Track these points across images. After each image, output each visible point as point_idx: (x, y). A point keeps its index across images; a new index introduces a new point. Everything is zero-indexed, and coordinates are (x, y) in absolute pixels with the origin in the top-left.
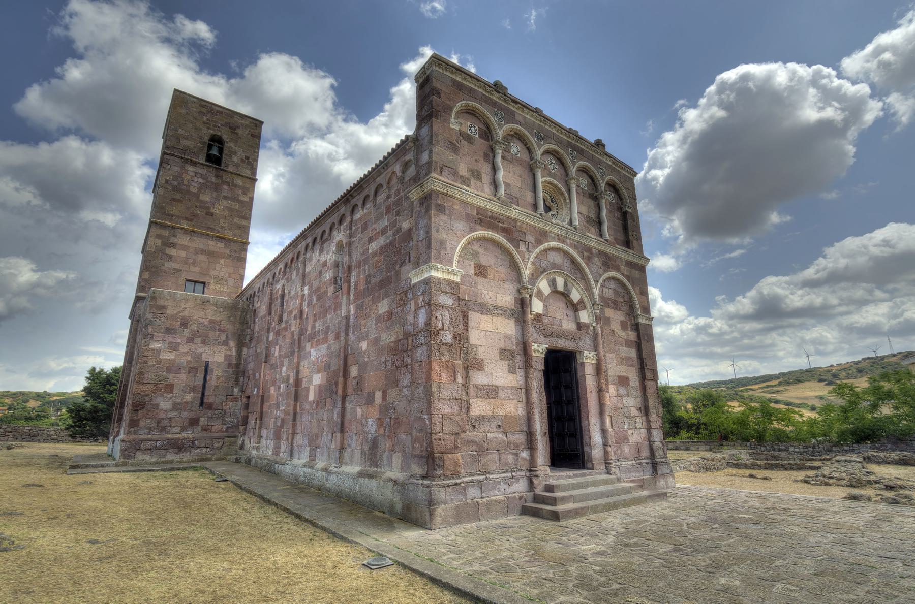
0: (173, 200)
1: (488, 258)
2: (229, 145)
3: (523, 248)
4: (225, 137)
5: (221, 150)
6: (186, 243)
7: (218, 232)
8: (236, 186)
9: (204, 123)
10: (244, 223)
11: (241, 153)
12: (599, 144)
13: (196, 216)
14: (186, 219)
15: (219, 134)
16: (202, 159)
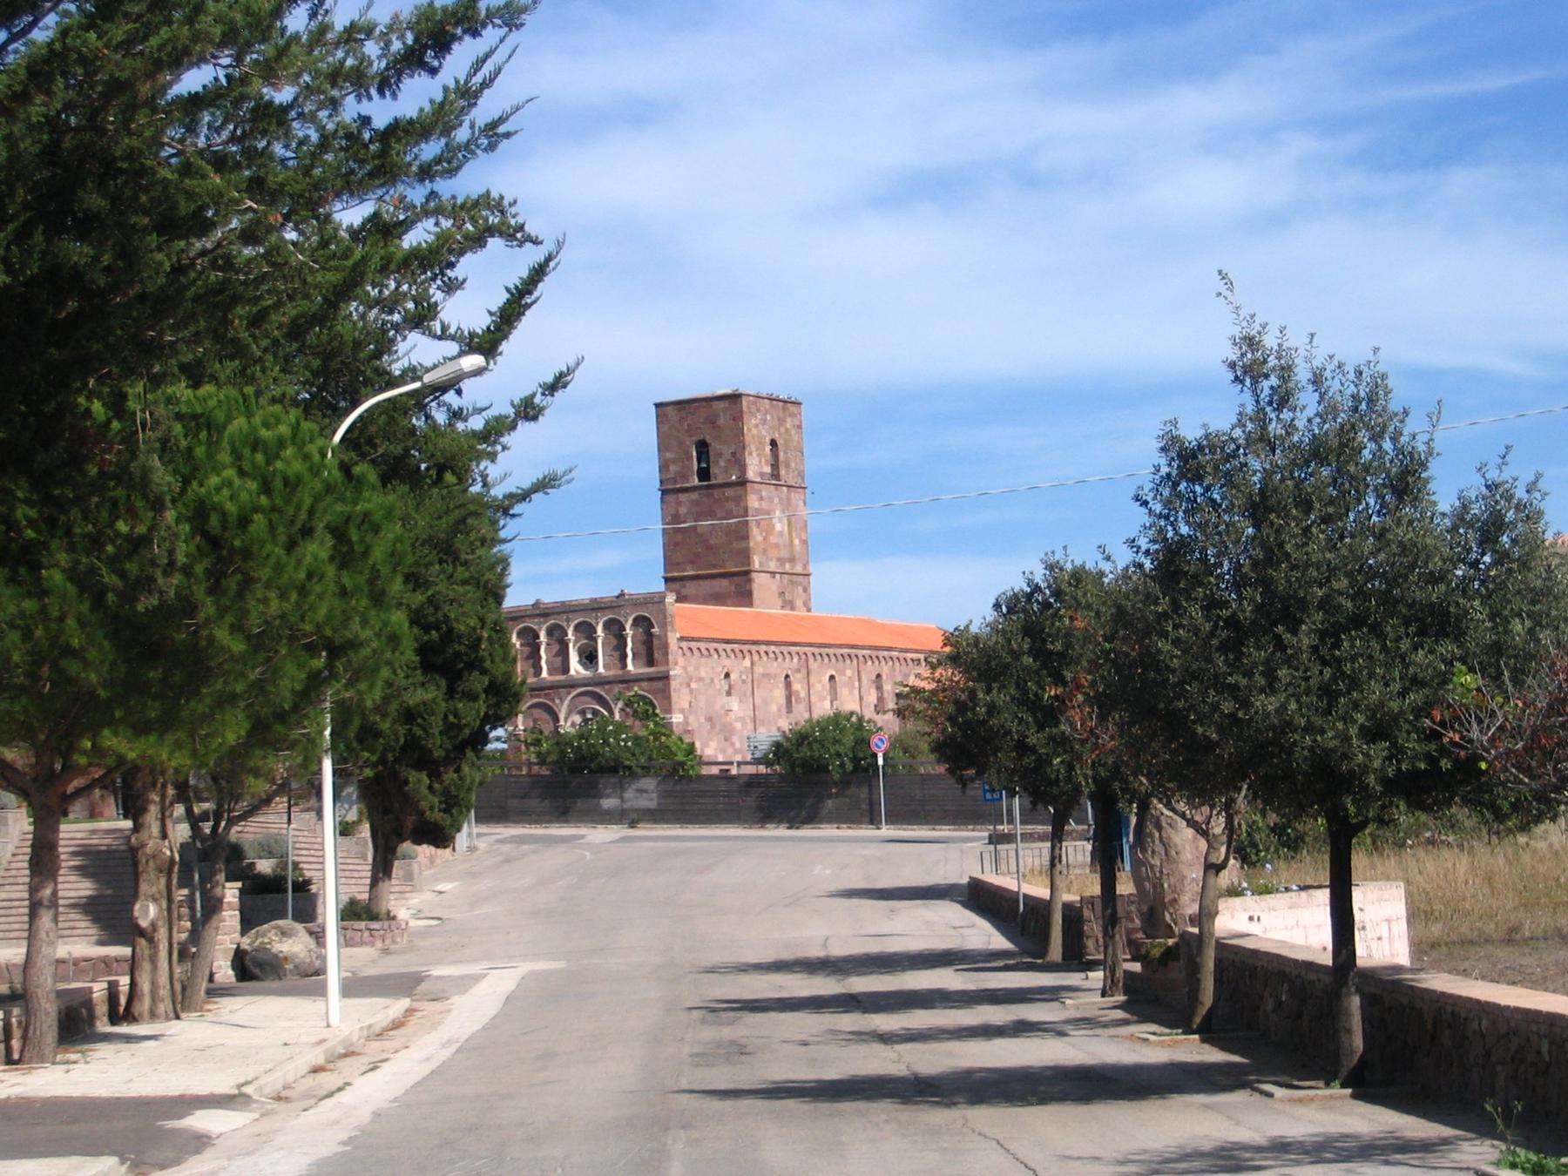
0: (676, 544)
1: (537, 712)
2: (715, 447)
3: (557, 701)
4: (708, 439)
5: (708, 463)
6: (694, 592)
7: (721, 567)
8: (727, 499)
9: (687, 431)
10: (743, 544)
11: (727, 451)
12: (622, 594)
13: (697, 555)
14: (692, 562)
15: (701, 437)
16: (696, 481)
